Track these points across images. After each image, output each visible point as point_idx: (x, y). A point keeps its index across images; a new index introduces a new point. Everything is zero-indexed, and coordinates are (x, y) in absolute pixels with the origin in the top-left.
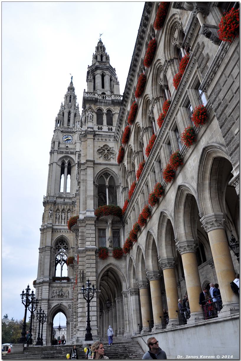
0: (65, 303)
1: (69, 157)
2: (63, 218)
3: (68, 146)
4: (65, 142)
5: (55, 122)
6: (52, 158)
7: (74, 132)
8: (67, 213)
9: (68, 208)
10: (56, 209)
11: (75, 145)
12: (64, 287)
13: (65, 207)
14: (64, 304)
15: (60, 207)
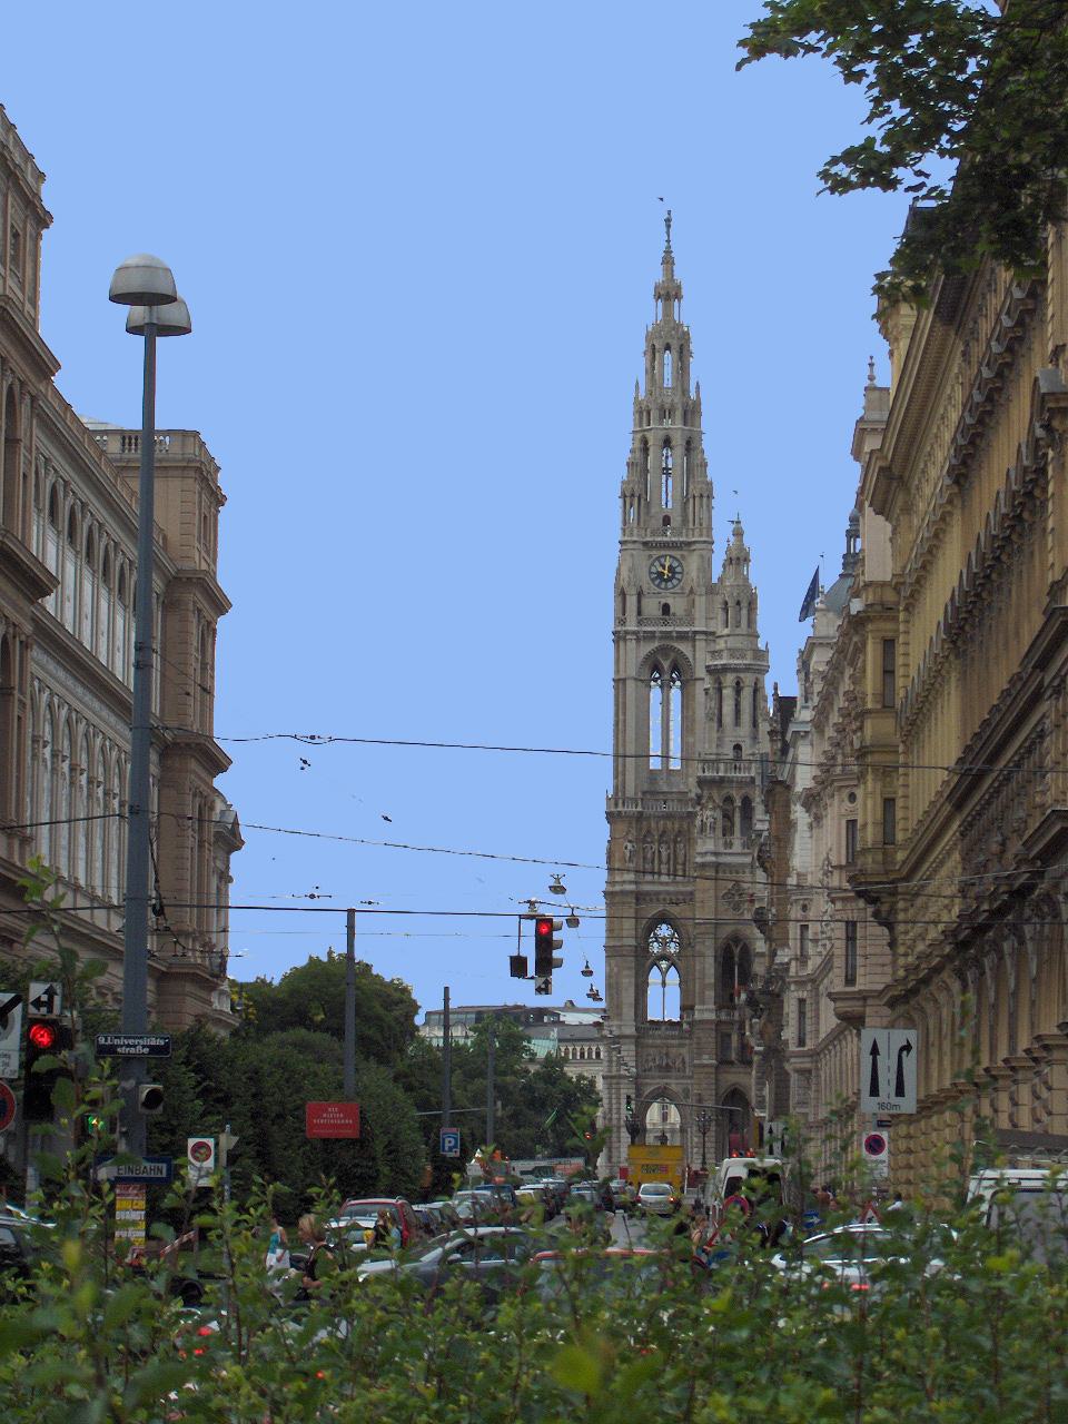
0: (674, 1085)
1: (673, 649)
2: (664, 859)
3: (670, 601)
4: (658, 586)
5: (620, 502)
6: (622, 652)
7: (690, 544)
8: (675, 842)
9: (677, 826)
10: (643, 833)
11: (692, 597)
12: (673, 1046)
13: (669, 824)
14: (673, 1087)
15: (653, 825)
